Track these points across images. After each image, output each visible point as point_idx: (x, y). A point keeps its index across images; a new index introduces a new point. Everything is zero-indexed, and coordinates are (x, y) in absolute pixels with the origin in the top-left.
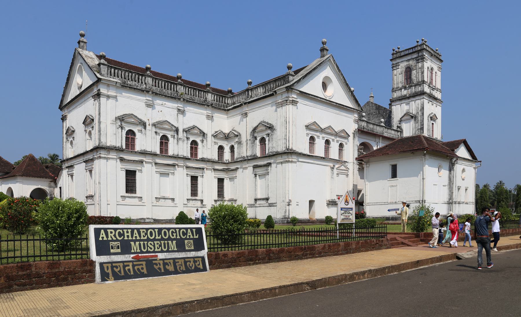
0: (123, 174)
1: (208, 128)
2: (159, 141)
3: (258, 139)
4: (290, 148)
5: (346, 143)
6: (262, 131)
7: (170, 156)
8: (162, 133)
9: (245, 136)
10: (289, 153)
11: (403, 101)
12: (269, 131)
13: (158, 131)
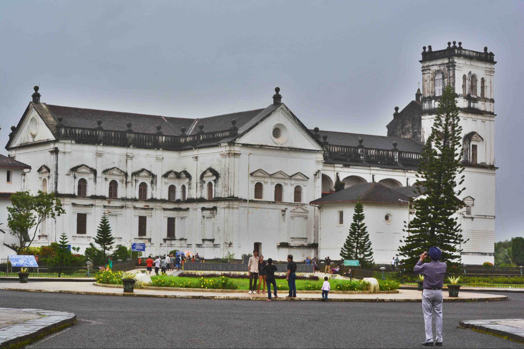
0: (75, 217)
1: (159, 171)
2: (108, 186)
3: (207, 183)
4: (232, 195)
6: (209, 177)
7: (118, 199)
8: (111, 178)
9: (195, 178)
10: (233, 199)
12: (214, 178)
13: (107, 176)
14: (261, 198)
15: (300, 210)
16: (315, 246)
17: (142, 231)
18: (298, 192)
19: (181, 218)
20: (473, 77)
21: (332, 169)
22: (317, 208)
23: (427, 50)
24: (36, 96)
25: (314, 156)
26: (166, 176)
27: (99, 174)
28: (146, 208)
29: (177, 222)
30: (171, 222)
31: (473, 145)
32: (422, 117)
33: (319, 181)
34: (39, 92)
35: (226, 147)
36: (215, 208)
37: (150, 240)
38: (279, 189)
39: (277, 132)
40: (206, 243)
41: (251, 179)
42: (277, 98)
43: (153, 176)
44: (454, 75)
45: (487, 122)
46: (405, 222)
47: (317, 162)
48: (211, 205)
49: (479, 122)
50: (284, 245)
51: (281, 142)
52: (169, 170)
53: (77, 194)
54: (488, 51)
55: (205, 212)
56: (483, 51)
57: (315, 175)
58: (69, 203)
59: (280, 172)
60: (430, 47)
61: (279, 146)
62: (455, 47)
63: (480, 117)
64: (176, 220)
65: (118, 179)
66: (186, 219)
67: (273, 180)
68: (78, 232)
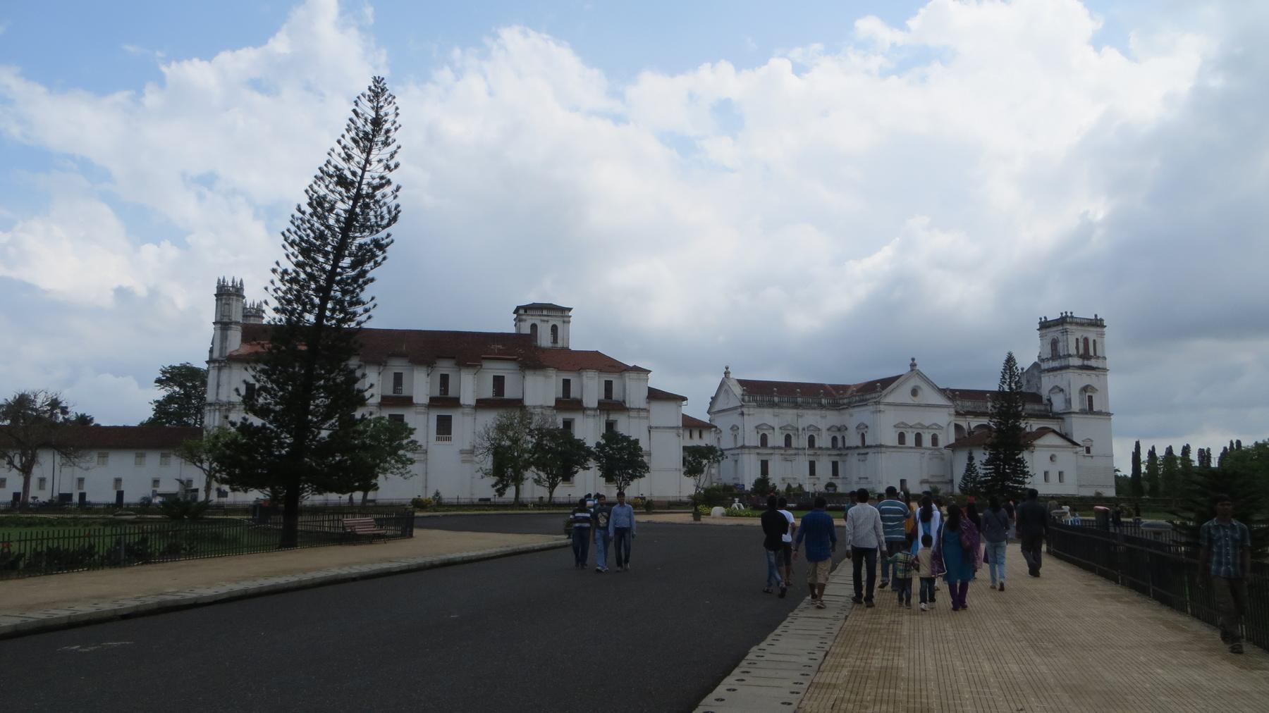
0: (760, 462)
3: (860, 433)
11: (1051, 373)
12: (866, 430)
14: (904, 444)
15: (937, 453)
16: (952, 481)
17: (812, 472)
18: (935, 440)
20: (1086, 340)
21: (964, 419)
22: (950, 451)
23: (1043, 320)
24: (727, 373)
25: (946, 410)
26: (828, 430)
27: (777, 429)
28: (815, 454)
30: (835, 465)
31: (1089, 396)
32: (1043, 375)
33: (952, 429)
34: (729, 370)
36: (867, 453)
37: (819, 479)
38: (918, 438)
39: (914, 392)
40: (862, 481)
42: (913, 365)
43: (819, 430)
44: (1067, 339)
45: (1102, 376)
46: (981, 461)
47: (950, 415)
49: (1093, 376)
50: (923, 482)
51: (917, 400)
52: (832, 425)
53: (760, 446)
54: (1098, 318)
55: (860, 456)
56: (1094, 318)
57: (949, 425)
59: (919, 424)
60: (1045, 318)
61: (917, 403)
62: (1067, 316)
63: (1093, 372)
64: (839, 463)
67: (913, 430)
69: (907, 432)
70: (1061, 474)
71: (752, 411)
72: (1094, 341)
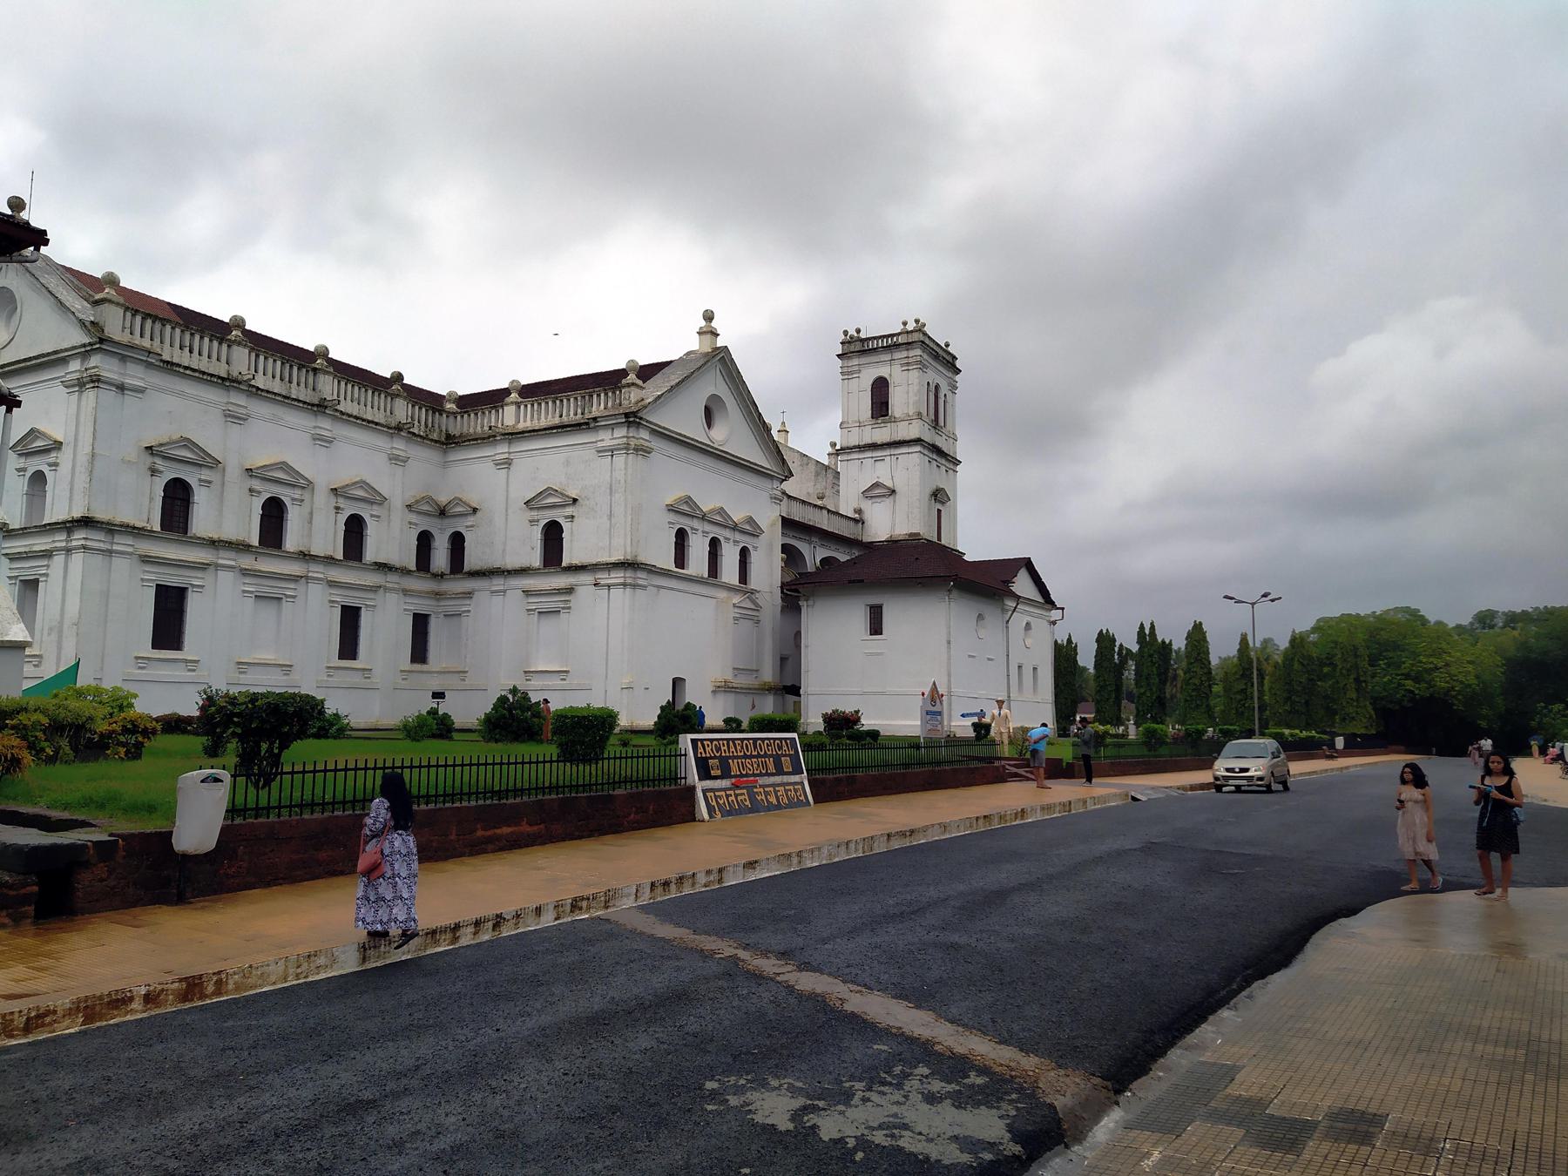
5: (755, 548)
11: (869, 454)
12: (569, 511)
17: (349, 647)
19: (445, 615)
20: (937, 387)
25: (767, 484)
29: (434, 627)
35: (613, 429)
36: (570, 590)
37: (366, 671)
41: (672, 517)
48: (561, 581)
49: (943, 468)
51: (719, 436)
58: (130, 550)
63: (943, 461)
65: (285, 494)
66: (464, 620)
67: (708, 527)
68: (156, 645)
69: (692, 529)
70: (1035, 669)
71: (134, 375)
72: (945, 395)
